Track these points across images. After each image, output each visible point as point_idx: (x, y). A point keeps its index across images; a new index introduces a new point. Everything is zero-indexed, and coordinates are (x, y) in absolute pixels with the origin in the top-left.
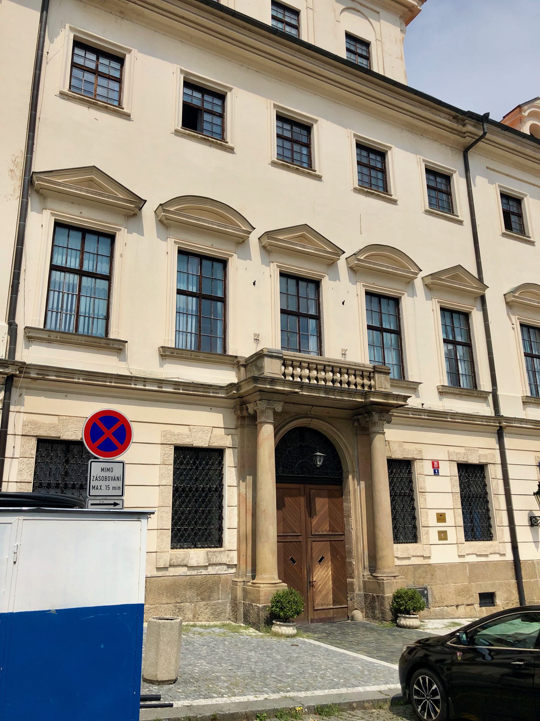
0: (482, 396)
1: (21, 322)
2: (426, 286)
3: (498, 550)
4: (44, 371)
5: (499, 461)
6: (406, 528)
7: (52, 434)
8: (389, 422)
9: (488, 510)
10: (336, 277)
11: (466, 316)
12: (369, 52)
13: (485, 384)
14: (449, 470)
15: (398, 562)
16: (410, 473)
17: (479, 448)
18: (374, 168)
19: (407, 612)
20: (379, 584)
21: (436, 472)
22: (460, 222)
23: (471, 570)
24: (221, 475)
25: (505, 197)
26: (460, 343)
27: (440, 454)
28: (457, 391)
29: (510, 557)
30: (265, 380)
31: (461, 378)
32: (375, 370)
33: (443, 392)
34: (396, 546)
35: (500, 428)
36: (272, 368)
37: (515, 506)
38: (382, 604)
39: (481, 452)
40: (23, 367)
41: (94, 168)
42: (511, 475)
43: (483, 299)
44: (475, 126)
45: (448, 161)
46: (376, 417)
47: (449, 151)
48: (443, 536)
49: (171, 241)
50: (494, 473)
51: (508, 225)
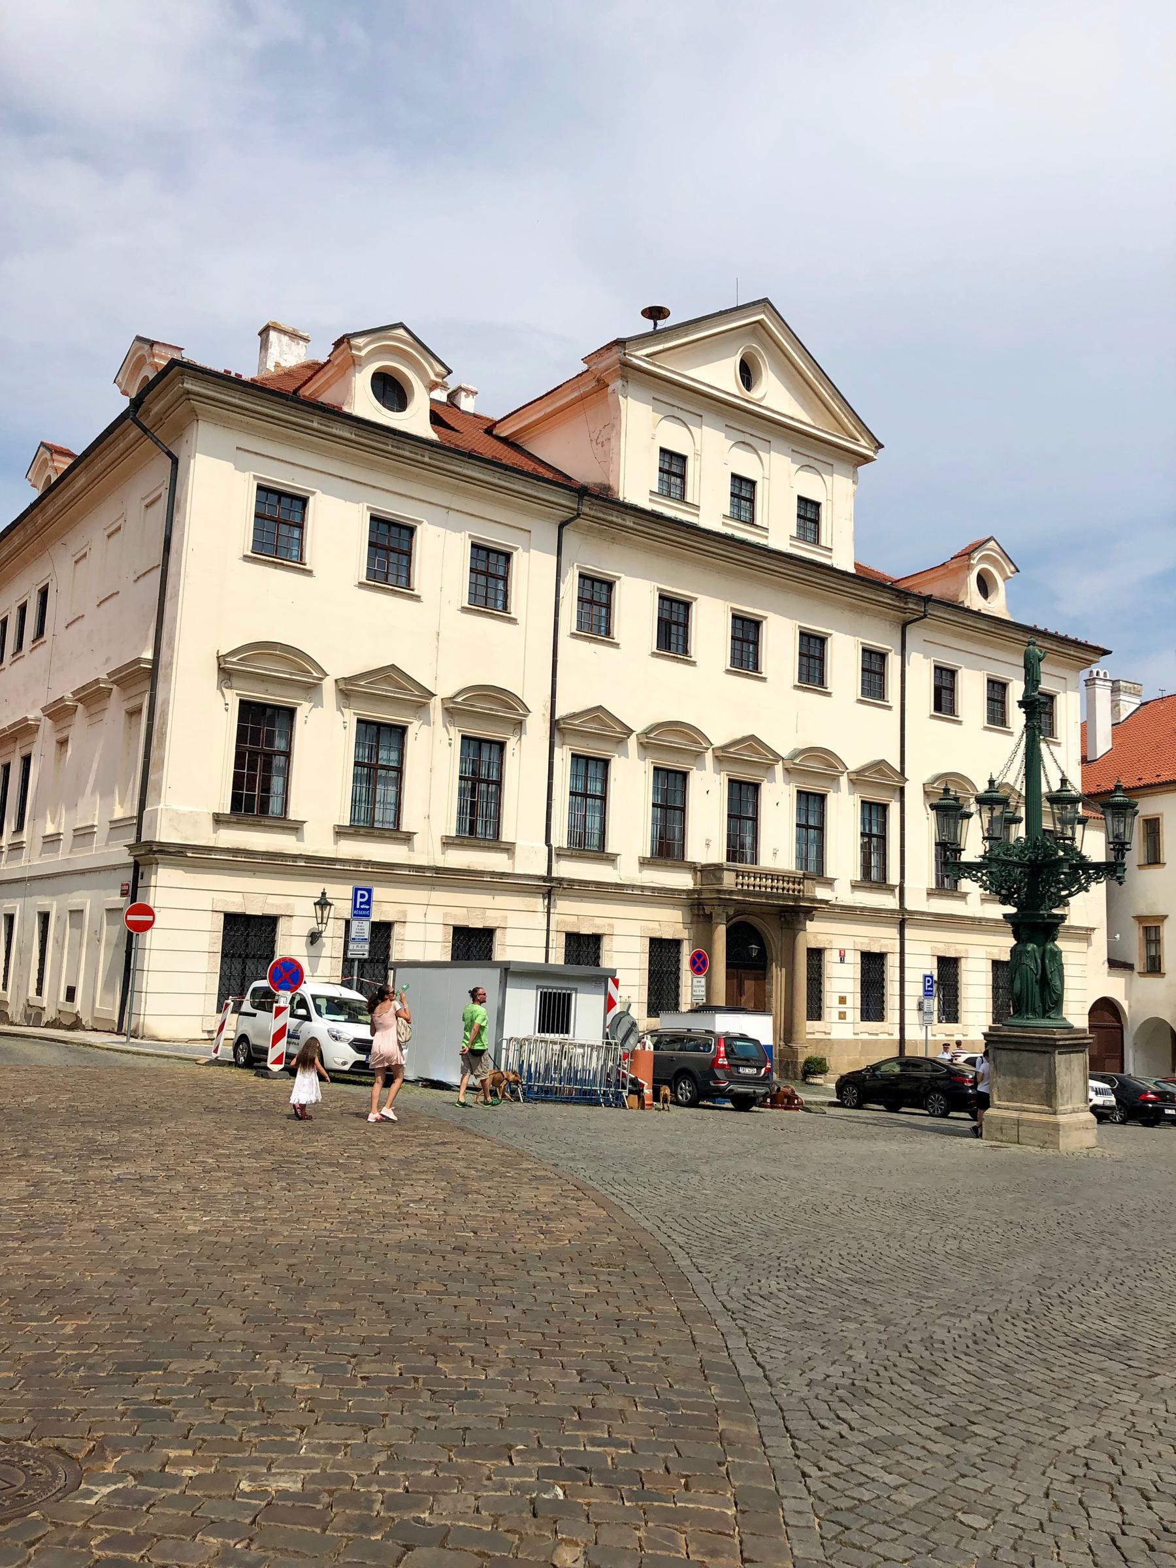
0: (890, 889)
1: (555, 843)
4: (572, 881)
5: (898, 950)
7: (575, 930)
8: (811, 920)
9: (883, 995)
10: (773, 780)
11: (884, 808)
12: (818, 514)
13: (894, 878)
14: (854, 959)
15: (809, 1037)
16: (820, 960)
17: (883, 938)
18: (813, 657)
19: (814, 1073)
20: (795, 1053)
21: (842, 961)
22: (889, 708)
24: (678, 961)
26: (875, 836)
27: (846, 943)
28: (868, 885)
29: (897, 1036)
30: (725, 892)
31: (873, 873)
32: (805, 877)
33: (855, 886)
34: (809, 1023)
36: (729, 880)
37: (907, 992)
38: (795, 1067)
39: (883, 942)
40: (560, 880)
41: (600, 708)
43: (902, 790)
44: (916, 604)
45: (884, 640)
47: (886, 626)
48: (842, 1016)
49: (649, 761)
50: (892, 961)
51: (938, 707)
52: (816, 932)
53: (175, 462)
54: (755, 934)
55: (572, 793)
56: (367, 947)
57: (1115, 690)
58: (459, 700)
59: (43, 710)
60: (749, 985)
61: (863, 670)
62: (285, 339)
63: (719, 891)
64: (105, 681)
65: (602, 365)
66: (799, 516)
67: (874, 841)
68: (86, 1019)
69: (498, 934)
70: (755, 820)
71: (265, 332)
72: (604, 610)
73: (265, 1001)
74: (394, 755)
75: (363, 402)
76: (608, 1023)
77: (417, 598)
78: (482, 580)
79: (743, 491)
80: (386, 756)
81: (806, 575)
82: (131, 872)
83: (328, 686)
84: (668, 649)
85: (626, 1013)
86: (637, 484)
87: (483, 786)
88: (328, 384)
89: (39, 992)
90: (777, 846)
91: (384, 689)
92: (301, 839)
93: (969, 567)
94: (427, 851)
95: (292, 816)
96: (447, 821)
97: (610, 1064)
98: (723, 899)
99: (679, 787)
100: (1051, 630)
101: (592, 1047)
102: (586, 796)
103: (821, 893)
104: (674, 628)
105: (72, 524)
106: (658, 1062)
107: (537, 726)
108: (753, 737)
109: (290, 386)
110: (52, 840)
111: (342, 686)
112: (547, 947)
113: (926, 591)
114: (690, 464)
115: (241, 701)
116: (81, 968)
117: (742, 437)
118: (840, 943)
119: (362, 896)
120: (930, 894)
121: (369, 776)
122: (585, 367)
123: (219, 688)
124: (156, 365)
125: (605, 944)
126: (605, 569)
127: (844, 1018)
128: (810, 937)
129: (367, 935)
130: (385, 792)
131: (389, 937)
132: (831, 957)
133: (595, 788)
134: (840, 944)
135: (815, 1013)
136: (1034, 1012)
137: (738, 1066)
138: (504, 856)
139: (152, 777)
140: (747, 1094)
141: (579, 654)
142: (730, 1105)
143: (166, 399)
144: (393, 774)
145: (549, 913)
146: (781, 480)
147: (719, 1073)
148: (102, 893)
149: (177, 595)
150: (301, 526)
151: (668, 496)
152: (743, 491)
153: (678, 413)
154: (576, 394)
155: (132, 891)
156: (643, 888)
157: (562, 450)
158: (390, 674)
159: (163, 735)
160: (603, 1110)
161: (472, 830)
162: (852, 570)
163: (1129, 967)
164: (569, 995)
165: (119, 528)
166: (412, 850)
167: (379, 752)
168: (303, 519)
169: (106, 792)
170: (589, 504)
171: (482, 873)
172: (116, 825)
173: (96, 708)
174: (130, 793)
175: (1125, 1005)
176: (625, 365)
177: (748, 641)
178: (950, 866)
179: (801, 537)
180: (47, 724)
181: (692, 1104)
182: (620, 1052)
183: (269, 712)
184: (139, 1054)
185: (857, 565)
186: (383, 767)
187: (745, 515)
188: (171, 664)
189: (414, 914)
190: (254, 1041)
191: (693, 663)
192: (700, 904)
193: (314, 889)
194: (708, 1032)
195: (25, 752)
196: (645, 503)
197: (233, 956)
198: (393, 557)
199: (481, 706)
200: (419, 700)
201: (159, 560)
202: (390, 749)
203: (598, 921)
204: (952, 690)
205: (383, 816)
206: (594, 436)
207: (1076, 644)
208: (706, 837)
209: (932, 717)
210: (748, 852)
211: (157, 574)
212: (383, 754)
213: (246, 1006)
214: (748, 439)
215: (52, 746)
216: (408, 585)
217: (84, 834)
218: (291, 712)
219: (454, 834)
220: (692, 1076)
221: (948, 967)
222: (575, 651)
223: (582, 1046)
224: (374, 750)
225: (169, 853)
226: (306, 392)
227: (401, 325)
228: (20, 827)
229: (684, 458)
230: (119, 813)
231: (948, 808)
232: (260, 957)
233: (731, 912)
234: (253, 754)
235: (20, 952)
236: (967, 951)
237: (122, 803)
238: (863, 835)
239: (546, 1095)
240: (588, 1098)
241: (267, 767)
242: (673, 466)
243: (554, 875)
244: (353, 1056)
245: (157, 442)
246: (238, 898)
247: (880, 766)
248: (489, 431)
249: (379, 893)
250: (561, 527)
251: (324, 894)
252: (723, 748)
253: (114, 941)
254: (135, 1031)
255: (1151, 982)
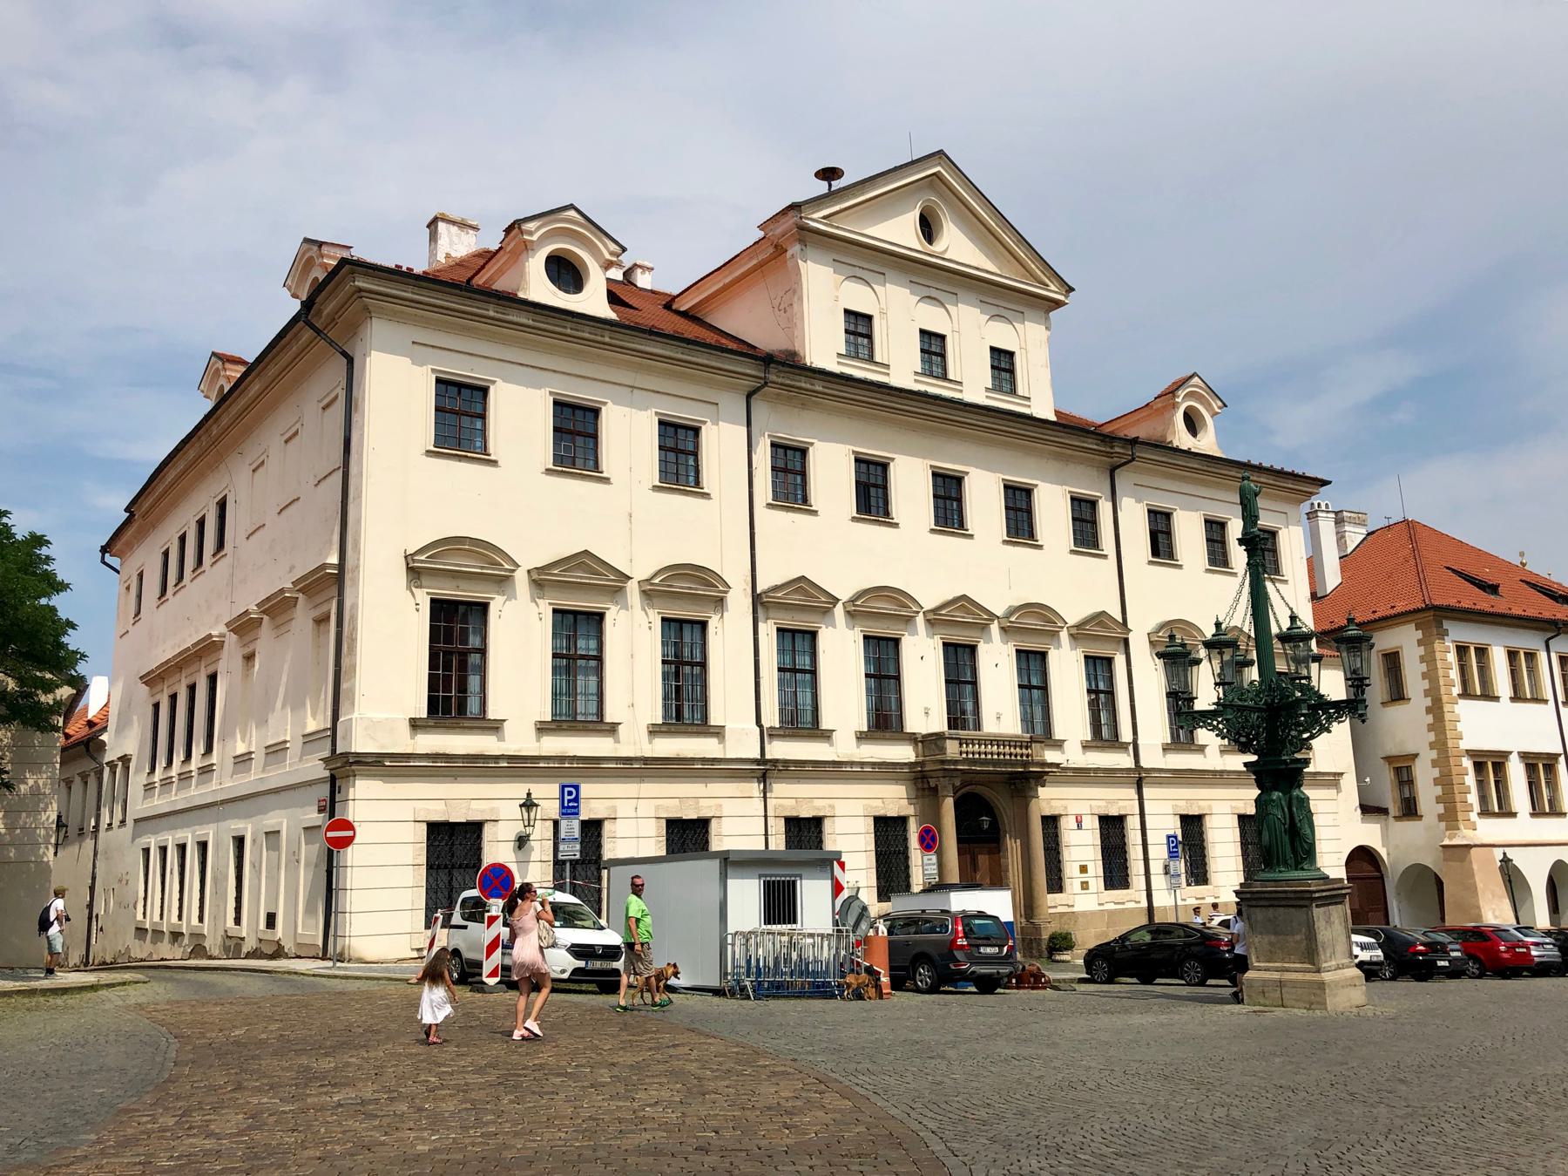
0: (1123, 747)
1: (766, 723)
2: (1071, 635)
3: (1132, 898)
4: (786, 762)
5: (1137, 811)
7: (795, 814)
10: (989, 640)
11: (1109, 661)
12: (1012, 364)
13: (1126, 735)
14: (1092, 824)
17: (1120, 800)
18: (1020, 510)
19: (1061, 950)
20: (1037, 929)
21: (1079, 827)
22: (1105, 557)
24: (906, 839)
25: (1153, 514)
27: (1082, 808)
29: (1144, 904)
31: (1104, 733)
32: (1032, 740)
33: (1086, 747)
35: (1139, 778)
37: (1151, 855)
38: (1039, 945)
39: (1121, 803)
40: (775, 762)
41: (803, 578)
42: (1148, 825)
43: (1126, 641)
45: (1092, 488)
46: (1033, 782)
47: (1094, 473)
48: (1085, 886)
49: (858, 629)
50: (1133, 824)
51: (1156, 552)
52: (1049, 798)
53: (350, 361)
54: (985, 804)
55: (780, 670)
56: (578, 847)
57: (1339, 521)
58: (656, 581)
59: (227, 625)
60: (983, 860)
61: (1074, 519)
62: (454, 229)
63: (943, 762)
64: (289, 590)
65: (779, 231)
66: (993, 367)
67: (1101, 697)
68: (288, 946)
69: (714, 824)
70: (974, 683)
71: (433, 224)
72: (799, 478)
73: (476, 911)
74: (593, 644)
75: (539, 287)
76: (837, 909)
77: (606, 480)
78: (671, 456)
79: (933, 346)
80: (584, 645)
81: (1004, 427)
82: (328, 786)
83: (521, 578)
84: (869, 512)
85: (854, 898)
86: (823, 347)
87: (687, 669)
88: (501, 272)
89: (238, 921)
90: (1000, 709)
91: (579, 576)
92: (501, 739)
93: (1175, 406)
94: (633, 742)
95: (491, 715)
96: (652, 708)
97: (843, 953)
98: (948, 770)
99: (892, 655)
100: (1266, 464)
101: (822, 936)
102: (794, 671)
103: (1051, 756)
104: (873, 491)
105: (248, 431)
106: (893, 948)
107: (739, 601)
108: (964, 597)
109: (462, 276)
110: (243, 760)
111: (535, 576)
112: (766, 834)
113: (1132, 433)
114: (876, 323)
115: (432, 601)
116: (281, 893)
117: (927, 292)
118: (1074, 808)
119: (570, 793)
120: (1166, 749)
121: (568, 666)
122: (762, 234)
123: (409, 588)
124: (325, 266)
125: (827, 826)
126: (797, 436)
128: (1043, 805)
129: (577, 834)
130: (585, 683)
131: (599, 835)
132: (1067, 824)
133: (803, 661)
134: (1075, 810)
135: (1056, 885)
136: (1286, 864)
137: (978, 946)
138: (714, 741)
139: (344, 686)
140: (991, 975)
141: (776, 524)
142: (974, 989)
143: (338, 299)
144: (593, 663)
145: (765, 798)
146: (972, 333)
147: (959, 955)
148: (299, 810)
149: (360, 497)
150: (483, 416)
151: (857, 357)
152: (933, 346)
153: (859, 273)
154: (754, 262)
155: (330, 806)
156: (862, 764)
157: (746, 320)
158: (584, 560)
159: (353, 640)
160: (838, 1002)
161: (679, 716)
162: (1053, 418)
163: (1383, 811)
164: (794, 883)
165: (296, 433)
166: (617, 741)
167: (578, 642)
168: (485, 409)
169: (296, 704)
170: (776, 373)
171: (693, 760)
172: (310, 739)
173: (280, 620)
174: (322, 704)
175: (1383, 852)
176: (803, 229)
177: (950, 498)
178: (1184, 717)
179: (997, 387)
180: (232, 639)
181: (933, 990)
182: (852, 939)
183: (462, 609)
184: (347, 977)
185: (1057, 413)
186: (583, 657)
187: (937, 370)
188: (358, 567)
189: (624, 809)
190: (467, 955)
191: (896, 525)
192: (923, 777)
193: (519, 790)
194: (943, 911)
195: (210, 670)
196: (833, 366)
197: (439, 867)
198: (580, 440)
199: (681, 586)
200: (615, 585)
201: (339, 462)
202: (588, 637)
203: (818, 803)
204: (1169, 533)
205: (585, 707)
206: (776, 303)
207: (1293, 476)
208: (924, 706)
209: (1151, 563)
210: (970, 717)
211: (339, 475)
212: (581, 643)
213: (457, 919)
214: (934, 293)
215: (239, 661)
216: (596, 467)
217: (276, 751)
218: (483, 608)
219: (660, 721)
220: (928, 960)
221: (1192, 825)
222: (773, 522)
223: (811, 935)
224: (572, 640)
225: (367, 764)
226: (479, 281)
227: (571, 207)
228: (209, 749)
229: (869, 318)
230: (312, 726)
231: (1176, 655)
232: (467, 866)
233: (958, 783)
234: (448, 653)
235: (215, 879)
236: (1210, 807)
237: (314, 716)
238: (1089, 691)
239: (778, 990)
240: (822, 991)
241: (463, 666)
242: (859, 326)
243: (768, 756)
244: (571, 963)
245: (331, 343)
246: (440, 806)
247: (1100, 618)
248: (668, 306)
249: (587, 789)
250: (749, 396)
251: (529, 794)
252: (935, 611)
253: (314, 859)
254: (342, 954)
255: (1408, 826)
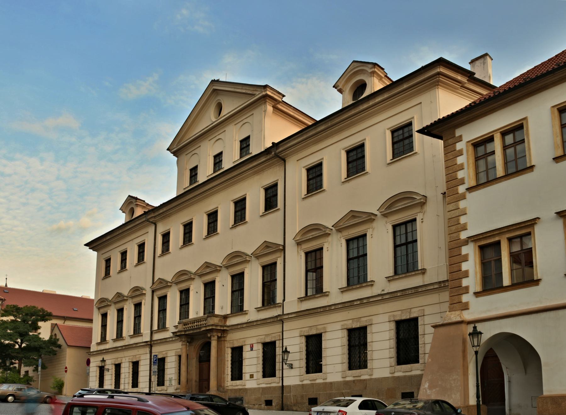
6: (237, 374)
14: (259, 349)
21: (252, 349)
23: (262, 390)
27: (253, 341)
39: (274, 335)
127: (253, 377)
132: (246, 349)
208: (196, 309)
236: (325, 328)
